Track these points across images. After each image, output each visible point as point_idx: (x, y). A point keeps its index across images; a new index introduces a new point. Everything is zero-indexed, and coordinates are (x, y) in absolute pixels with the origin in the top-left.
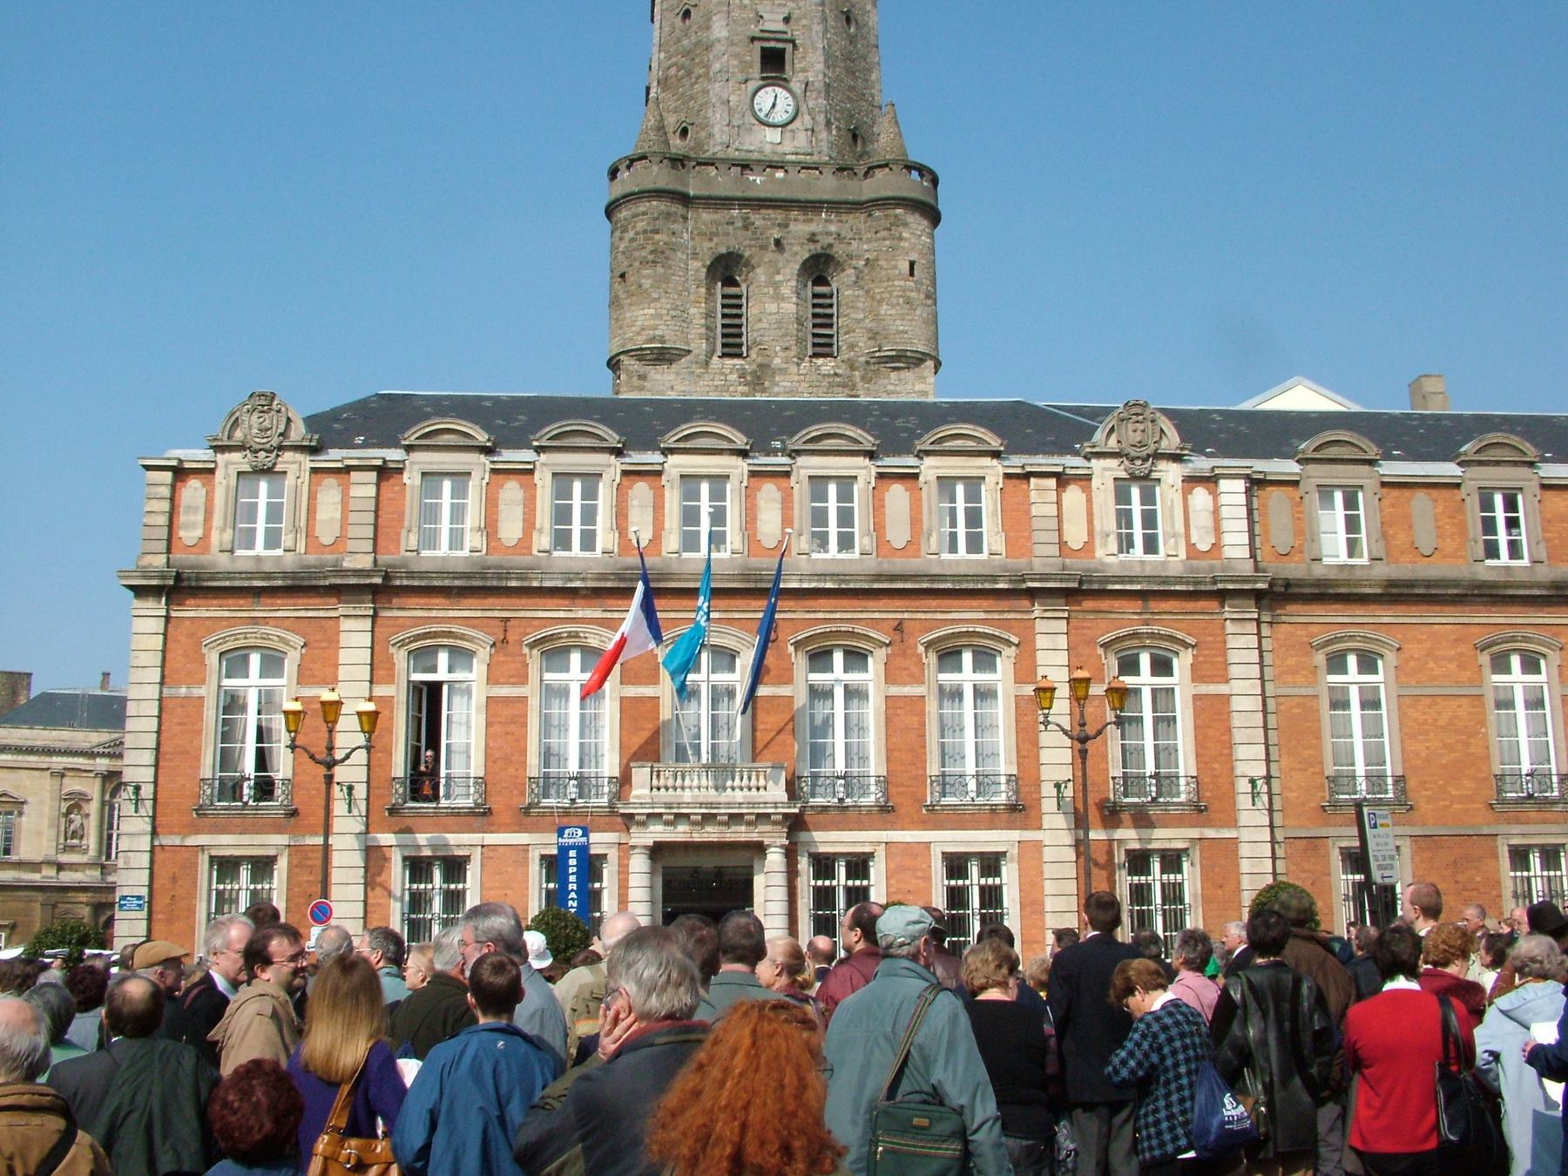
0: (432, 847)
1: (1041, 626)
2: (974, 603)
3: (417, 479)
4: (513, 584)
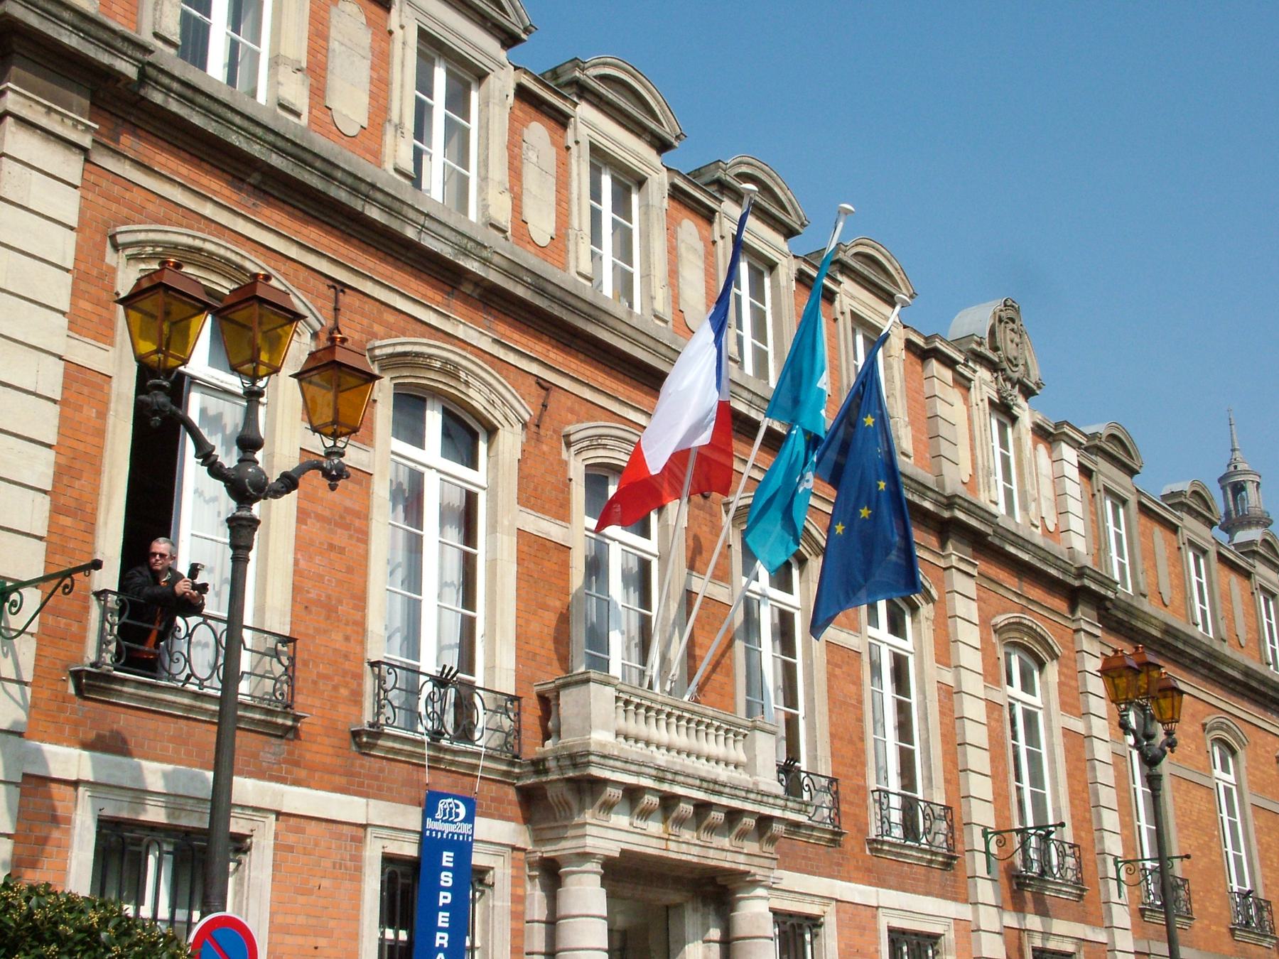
4: (374, 213)
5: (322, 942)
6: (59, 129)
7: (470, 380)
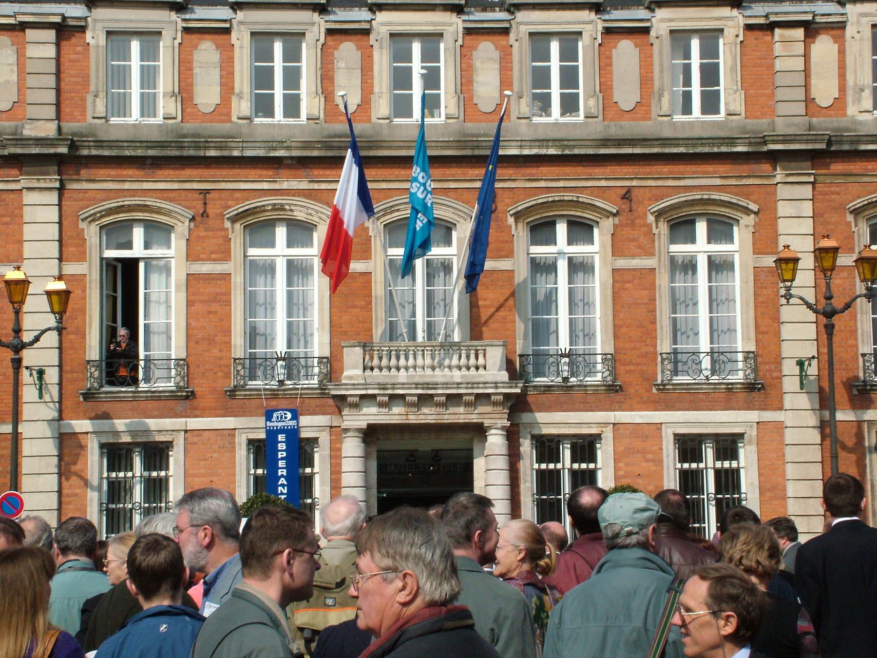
0: (131, 432)
1: (783, 192)
2: (710, 168)
3: (102, 39)
4: (212, 153)
5: (214, 479)
6: (44, 185)
7: (292, 208)
